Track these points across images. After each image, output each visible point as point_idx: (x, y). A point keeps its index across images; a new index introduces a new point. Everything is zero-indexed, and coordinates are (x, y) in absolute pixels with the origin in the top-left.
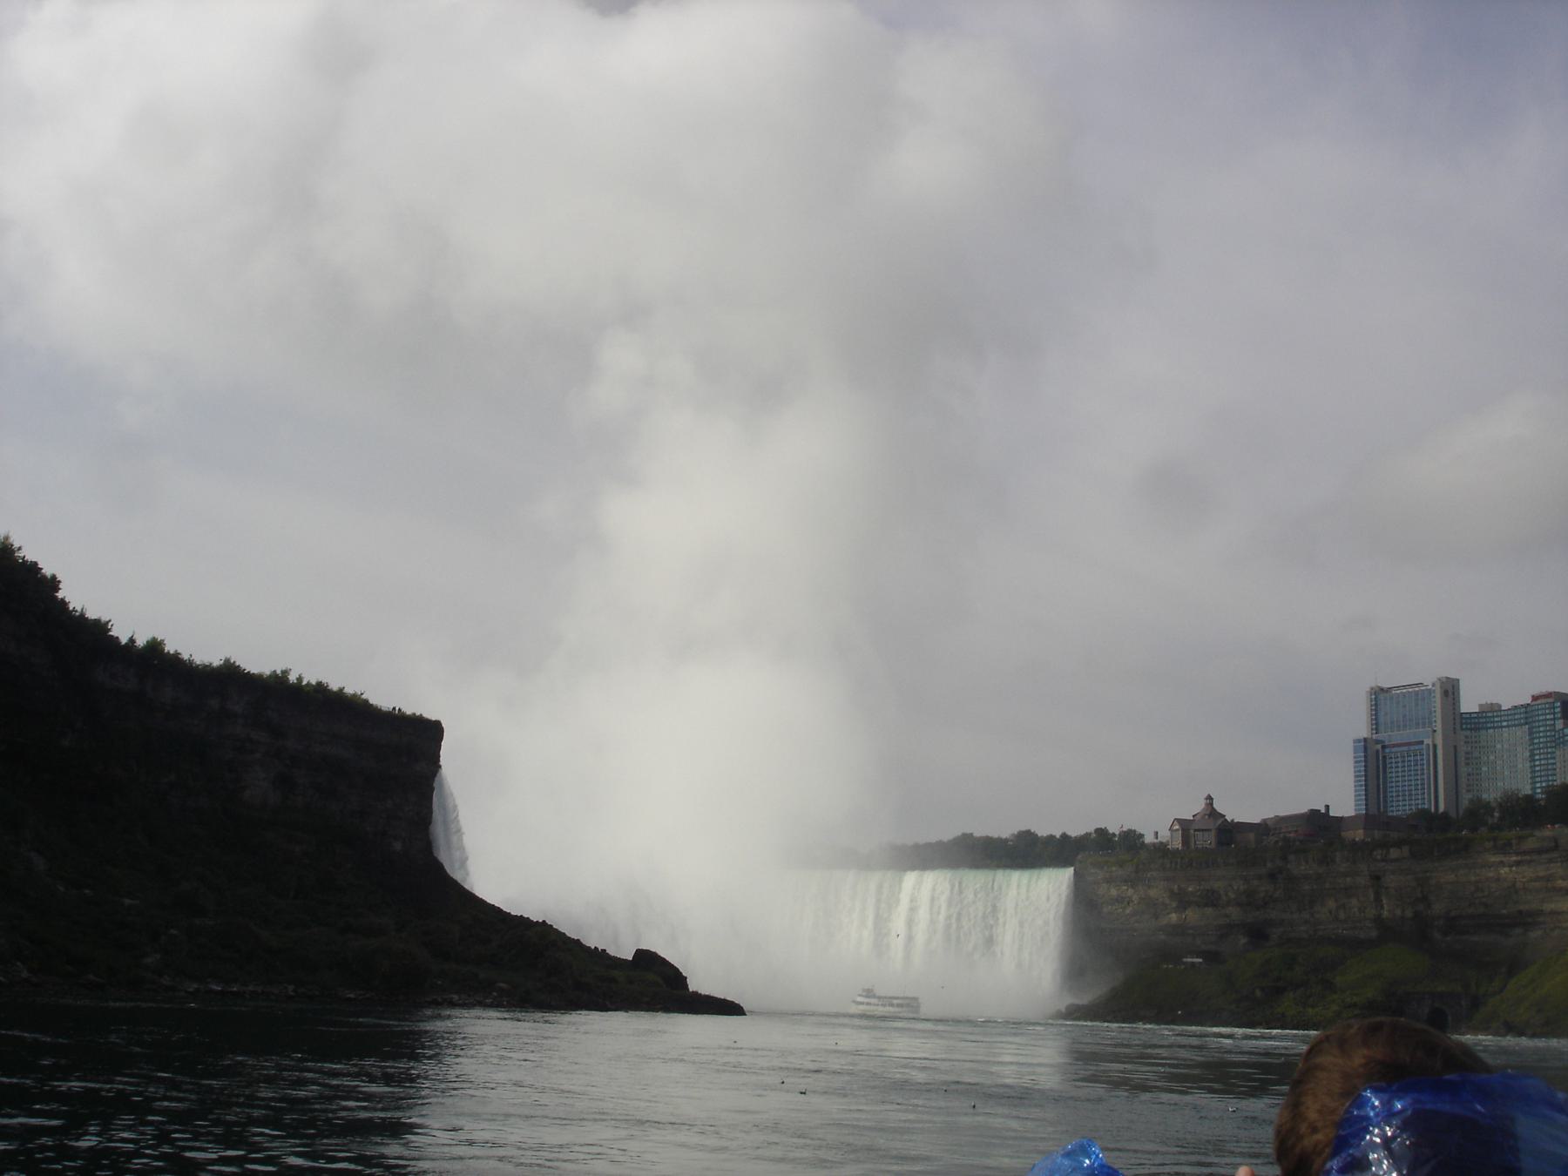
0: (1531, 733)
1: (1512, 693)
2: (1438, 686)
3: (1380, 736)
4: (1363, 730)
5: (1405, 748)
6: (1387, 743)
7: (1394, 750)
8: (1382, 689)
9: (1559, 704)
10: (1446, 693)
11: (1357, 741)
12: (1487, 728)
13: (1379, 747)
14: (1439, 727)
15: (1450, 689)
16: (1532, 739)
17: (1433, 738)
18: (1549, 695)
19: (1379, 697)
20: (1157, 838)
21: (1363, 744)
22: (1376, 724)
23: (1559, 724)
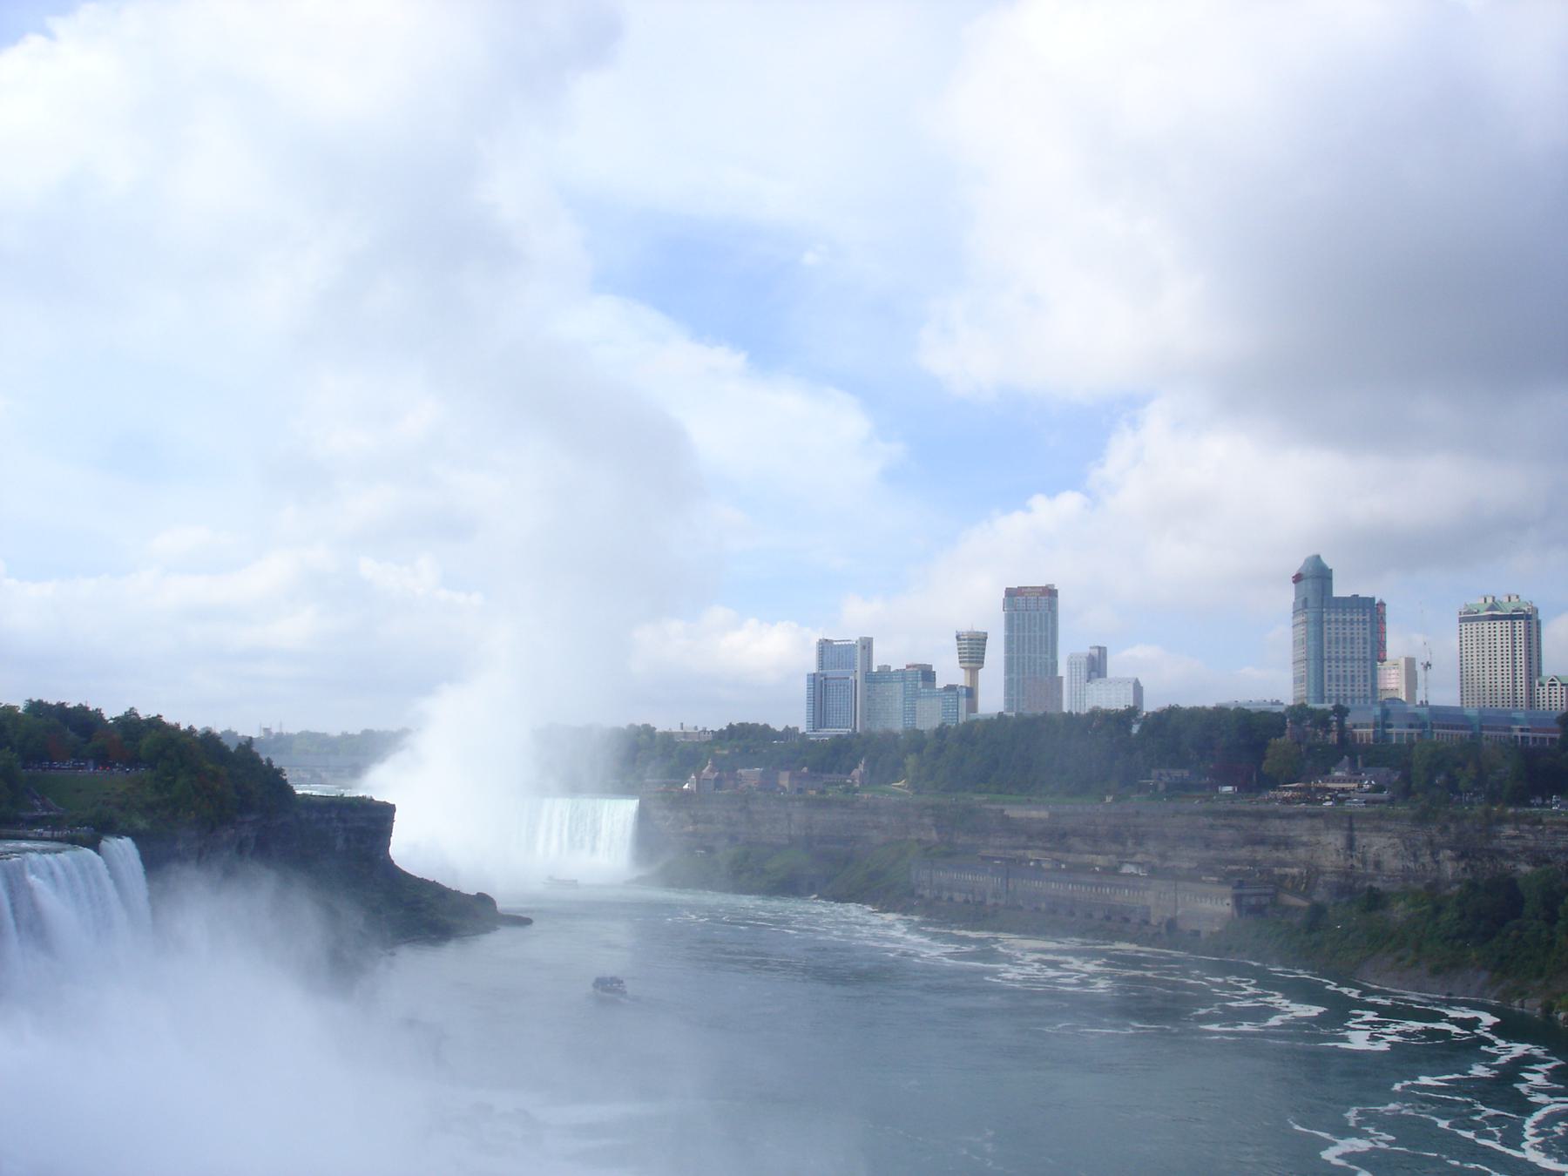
0: (905, 688)
2: (859, 644)
3: (824, 671)
4: (814, 669)
5: (837, 681)
6: (828, 677)
7: (833, 681)
8: (827, 640)
9: (920, 672)
10: (864, 648)
12: (880, 682)
13: (823, 678)
14: (858, 668)
15: (867, 645)
16: (905, 692)
17: (855, 677)
18: (915, 666)
19: (825, 647)
20: (682, 728)
21: (812, 677)
22: (821, 665)
23: (920, 684)
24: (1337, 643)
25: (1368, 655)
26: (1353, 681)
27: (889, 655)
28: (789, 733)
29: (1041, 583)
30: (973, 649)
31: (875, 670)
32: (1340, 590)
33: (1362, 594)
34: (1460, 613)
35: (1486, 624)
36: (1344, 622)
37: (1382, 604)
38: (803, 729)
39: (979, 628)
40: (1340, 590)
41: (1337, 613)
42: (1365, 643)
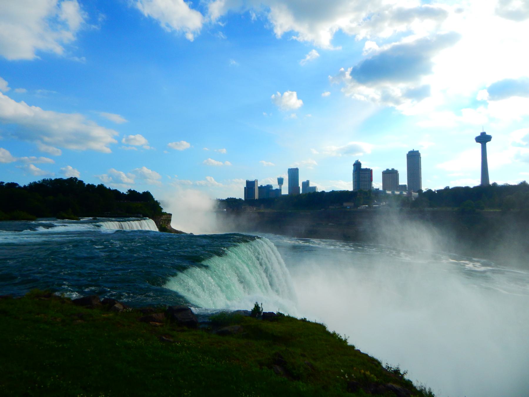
1: (264, 185)
4: (245, 186)
11: (245, 187)
18: (269, 185)
24: (363, 177)
25: (369, 180)
26: (366, 185)
27: (262, 182)
28: (240, 199)
29: (295, 167)
30: (280, 181)
31: (259, 185)
32: (363, 167)
33: (368, 168)
34: (382, 172)
35: (388, 174)
36: (364, 173)
37: (372, 170)
38: (243, 198)
39: (282, 177)
40: (363, 167)
41: (364, 172)
42: (369, 177)
